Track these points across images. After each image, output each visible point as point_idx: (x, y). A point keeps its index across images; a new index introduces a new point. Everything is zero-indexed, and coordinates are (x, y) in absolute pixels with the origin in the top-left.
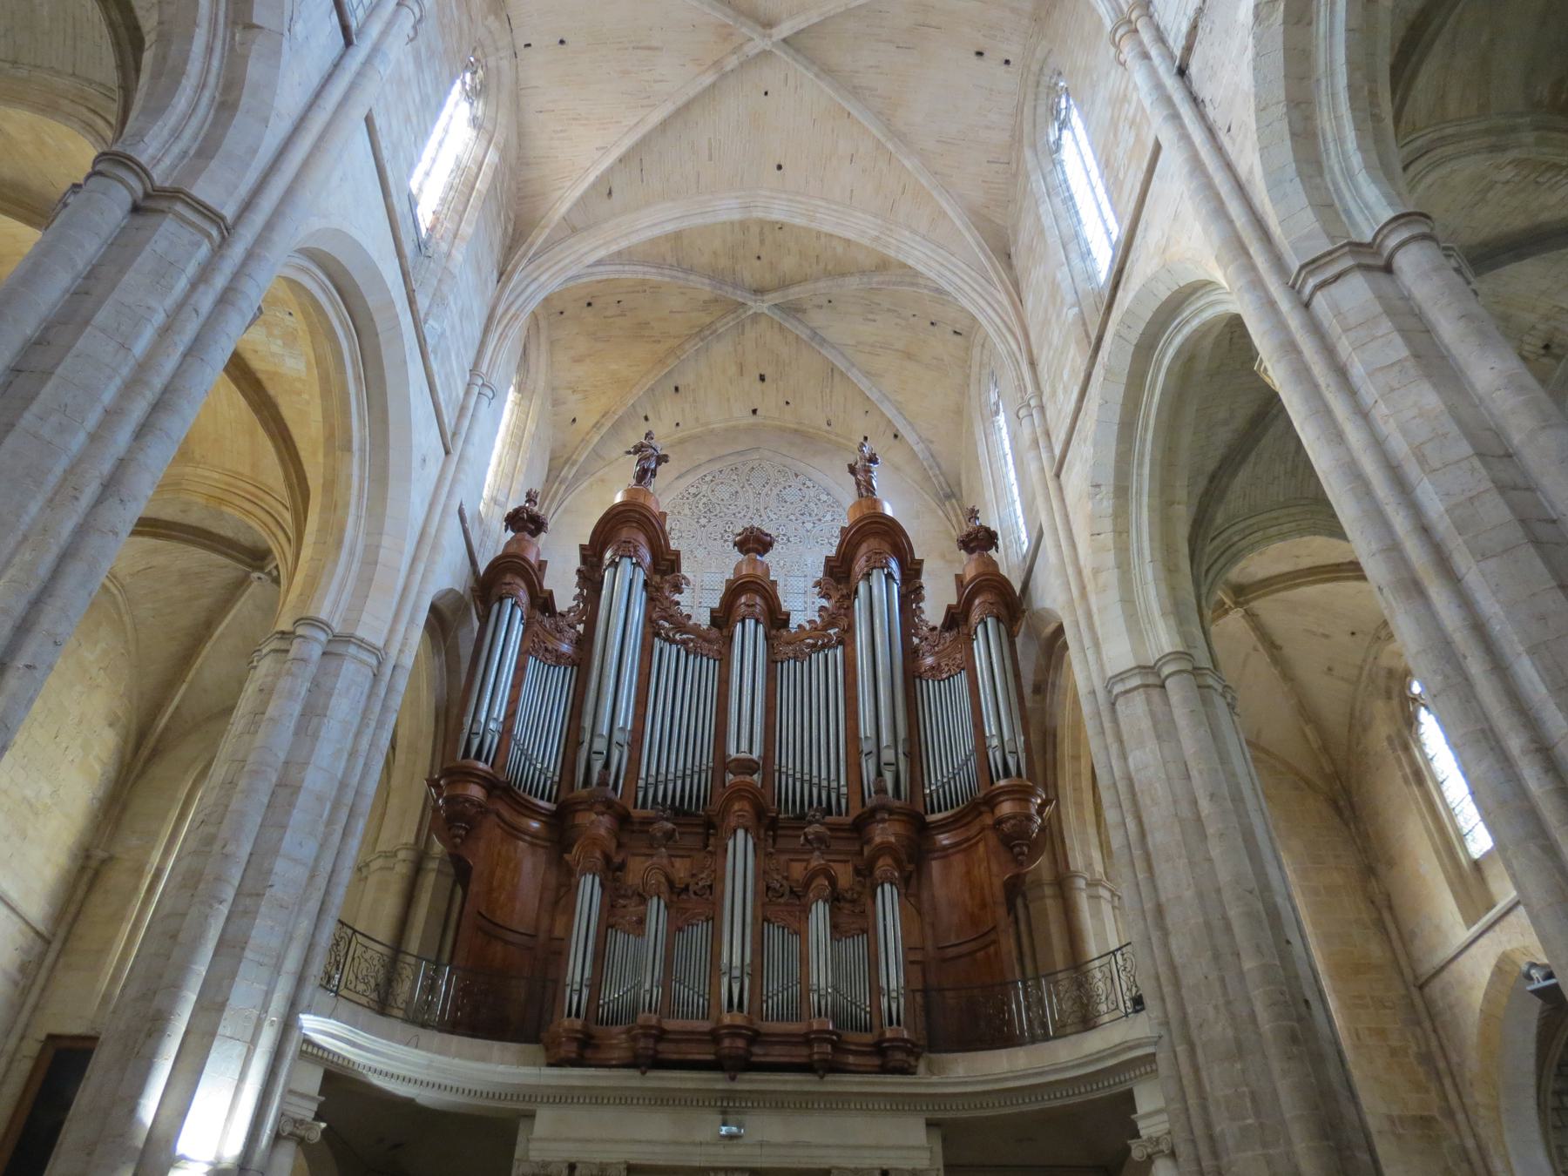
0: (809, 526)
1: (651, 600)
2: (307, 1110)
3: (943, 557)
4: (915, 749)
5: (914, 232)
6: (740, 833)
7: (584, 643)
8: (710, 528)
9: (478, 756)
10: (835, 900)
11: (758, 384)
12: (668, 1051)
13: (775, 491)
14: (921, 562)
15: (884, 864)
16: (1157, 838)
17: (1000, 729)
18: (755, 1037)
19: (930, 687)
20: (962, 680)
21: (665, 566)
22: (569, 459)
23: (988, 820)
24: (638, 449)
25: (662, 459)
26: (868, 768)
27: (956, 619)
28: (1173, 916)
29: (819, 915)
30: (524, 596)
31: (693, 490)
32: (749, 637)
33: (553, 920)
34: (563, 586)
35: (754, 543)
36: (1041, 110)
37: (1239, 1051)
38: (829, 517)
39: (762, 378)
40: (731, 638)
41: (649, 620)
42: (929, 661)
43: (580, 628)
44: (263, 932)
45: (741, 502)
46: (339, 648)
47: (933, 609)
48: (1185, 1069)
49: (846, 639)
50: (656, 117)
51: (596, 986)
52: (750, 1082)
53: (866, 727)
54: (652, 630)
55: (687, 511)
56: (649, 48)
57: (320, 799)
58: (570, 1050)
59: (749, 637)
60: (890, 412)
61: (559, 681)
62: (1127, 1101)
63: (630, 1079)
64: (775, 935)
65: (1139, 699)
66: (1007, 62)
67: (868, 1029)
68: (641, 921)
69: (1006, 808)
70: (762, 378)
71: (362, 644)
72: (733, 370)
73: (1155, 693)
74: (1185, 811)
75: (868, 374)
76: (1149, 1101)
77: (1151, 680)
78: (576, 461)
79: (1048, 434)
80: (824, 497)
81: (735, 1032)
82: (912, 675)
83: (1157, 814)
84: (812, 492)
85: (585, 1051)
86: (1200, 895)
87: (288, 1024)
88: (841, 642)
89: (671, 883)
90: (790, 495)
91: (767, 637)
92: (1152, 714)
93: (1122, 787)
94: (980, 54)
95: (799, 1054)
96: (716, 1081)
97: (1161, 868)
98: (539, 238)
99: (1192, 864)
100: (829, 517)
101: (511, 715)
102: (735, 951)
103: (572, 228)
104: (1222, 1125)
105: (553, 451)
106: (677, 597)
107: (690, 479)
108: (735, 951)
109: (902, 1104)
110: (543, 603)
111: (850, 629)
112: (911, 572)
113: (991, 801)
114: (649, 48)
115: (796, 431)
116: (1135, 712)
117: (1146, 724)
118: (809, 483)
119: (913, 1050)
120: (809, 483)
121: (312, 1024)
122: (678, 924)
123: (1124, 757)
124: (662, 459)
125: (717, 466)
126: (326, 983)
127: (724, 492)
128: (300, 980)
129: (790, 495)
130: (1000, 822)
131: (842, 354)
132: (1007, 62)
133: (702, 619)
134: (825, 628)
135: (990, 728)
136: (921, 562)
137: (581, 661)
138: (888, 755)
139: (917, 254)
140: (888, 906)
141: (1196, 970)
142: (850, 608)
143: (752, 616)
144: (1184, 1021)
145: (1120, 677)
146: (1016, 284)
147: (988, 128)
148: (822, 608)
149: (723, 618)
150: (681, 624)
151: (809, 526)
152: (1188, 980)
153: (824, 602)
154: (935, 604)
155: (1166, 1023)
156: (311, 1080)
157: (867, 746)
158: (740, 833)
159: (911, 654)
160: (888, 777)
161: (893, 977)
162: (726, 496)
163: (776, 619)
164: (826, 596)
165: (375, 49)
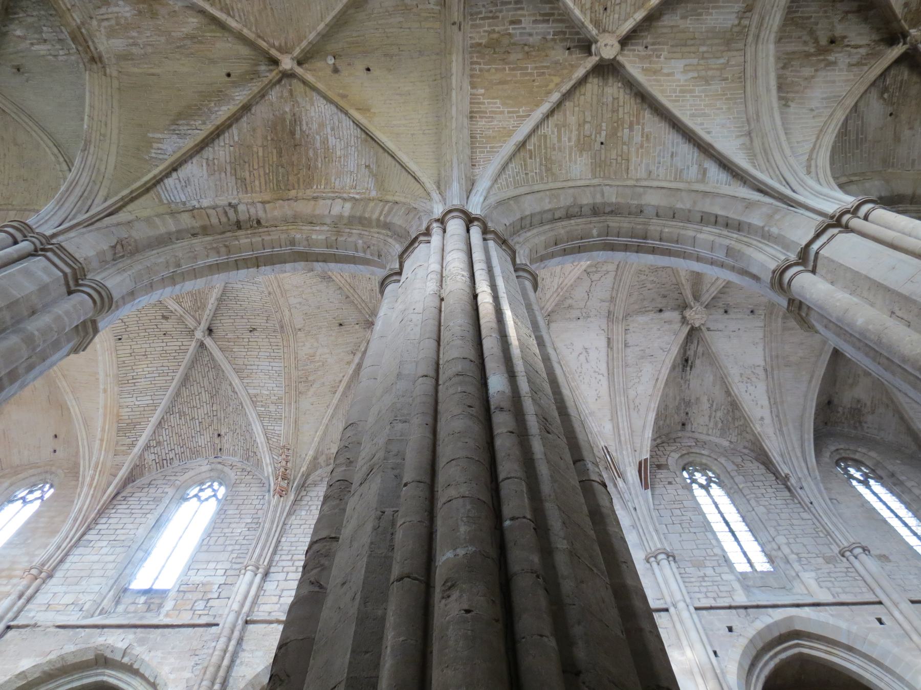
36: (33, 479)
66: (55, 451)
94: (56, 436)
132: (55, 451)
147: (19, 452)
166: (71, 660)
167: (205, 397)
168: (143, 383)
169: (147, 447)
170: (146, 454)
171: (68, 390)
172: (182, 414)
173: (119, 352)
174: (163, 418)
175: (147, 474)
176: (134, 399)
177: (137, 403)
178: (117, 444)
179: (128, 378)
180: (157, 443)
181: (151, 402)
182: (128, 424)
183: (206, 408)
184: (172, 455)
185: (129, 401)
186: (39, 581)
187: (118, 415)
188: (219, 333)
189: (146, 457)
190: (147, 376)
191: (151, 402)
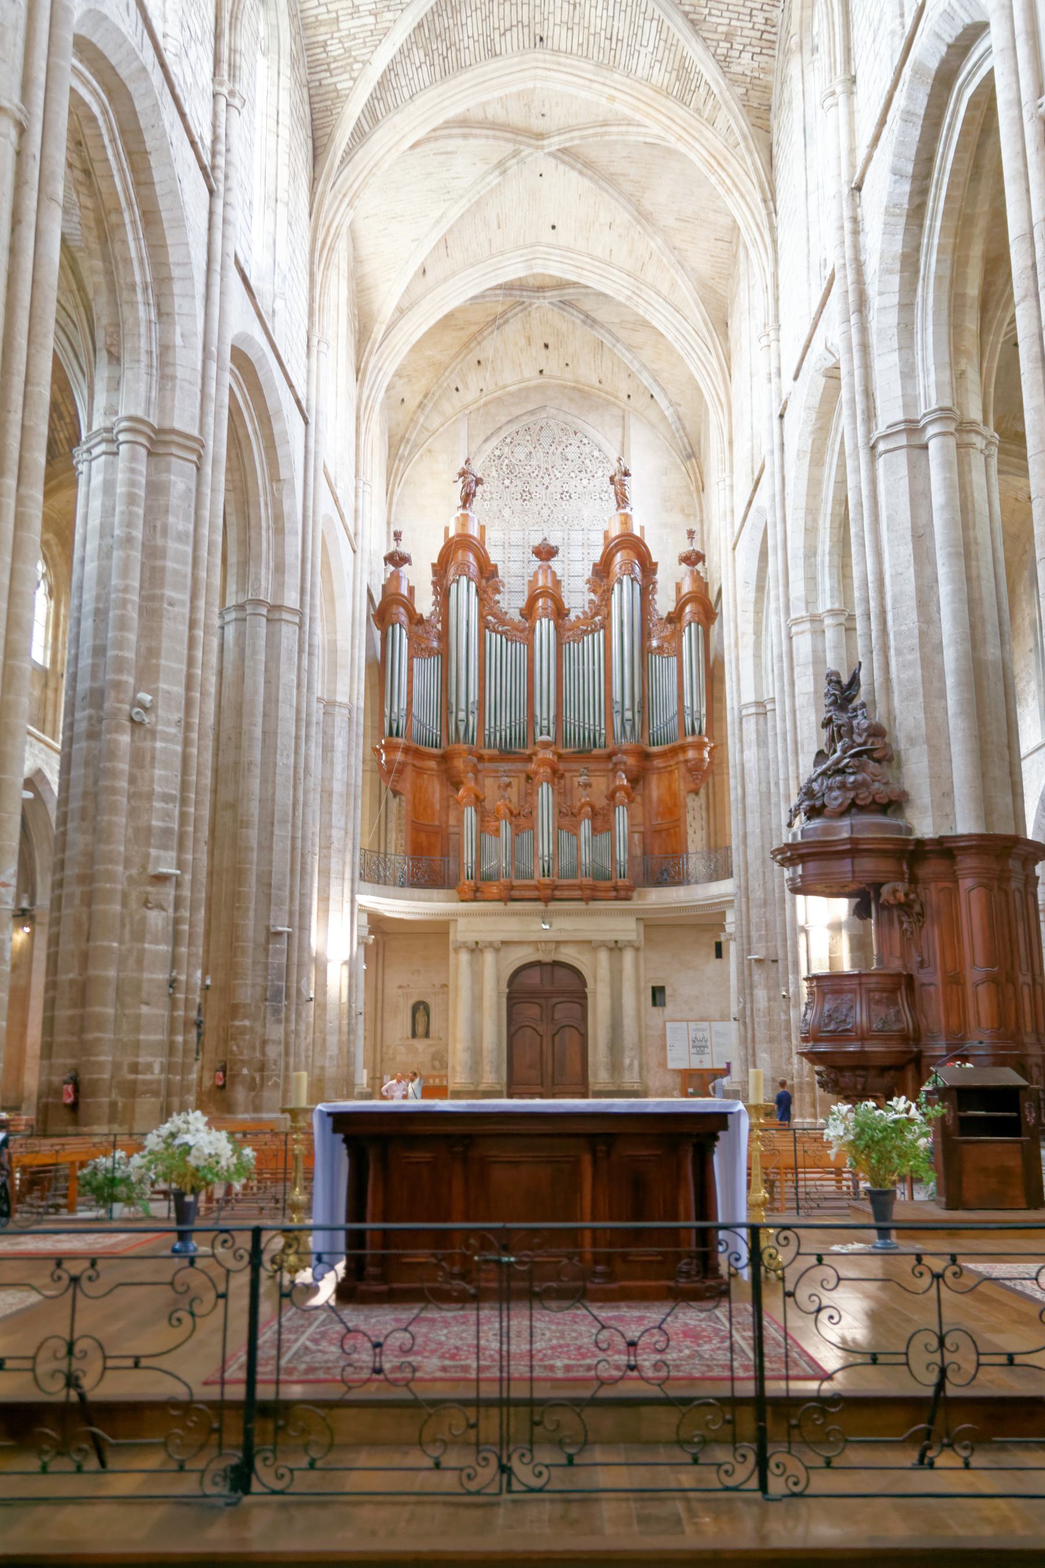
0: (585, 482)
1: (481, 600)
2: (365, 932)
3: (682, 510)
4: (645, 705)
5: (658, 293)
6: (545, 785)
7: (444, 636)
8: (512, 489)
9: (397, 734)
10: (594, 814)
11: (543, 350)
12: (515, 893)
13: (560, 450)
14: (656, 564)
15: (620, 795)
16: (749, 800)
17: (695, 702)
18: (556, 888)
19: (657, 661)
20: (674, 661)
22: (403, 437)
23: (681, 758)
24: (463, 474)
25: (479, 482)
27: (675, 618)
28: (750, 840)
29: (585, 827)
30: (404, 619)
31: (497, 453)
32: (544, 628)
33: (448, 815)
34: (425, 605)
35: (546, 553)
37: (765, 903)
38: (600, 474)
39: (546, 346)
40: (534, 630)
41: (481, 617)
42: (655, 643)
43: (439, 626)
44: (335, 865)
45: (534, 463)
46: (276, 616)
47: (664, 603)
48: (744, 909)
49: (606, 625)
50: (455, 213)
51: (478, 863)
52: (553, 906)
53: (617, 696)
54: (484, 625)
55: (494, 474)
56: (447, 153)
57: (341, 796)
58: (470, 895)
59: (544, 628)
60: (646, 380)
61: (432, 664)
62: (723, 914)
63: (498, 906)
64: (564, 834)
65: (753, 720)
67: (610, 879)
68: (497, 830)
69: (691, 754)
70: (546, 346)
71: (341, 705)
72: (523, 342)
73: (761, 718)
74: (764, 789)
75: (629, 348)
76: (730, 917)
77: (761, 710)
78: (408, 440)
79: (732, 511)
80: (596, 453)
81: (546, 886)
82: (645, 651)
83: (752, 787)
84: (587, 449)
85: (476, 895)
86: (762, 832)
87: (353, 901)
88: (603, 627)
89: (511, 813)
90: (572, 452)
91: (556, 627)
92: (758, 731)
93: (738, 768)
95: (577, 893)
96: (539, 906)
97: (749, 815)
98: (378, 331)
99: (761, 816)
100: (600, 474)
101: (410, 703)
102: (545, 847)
103: (401, 312)
104: (754, 934)
105: (390, 430)
106: (497, 597)
107: (495, 442)
108: (545, 847)
109: (624, 913)
110: (416, 620)
111: (608, 617)
112: (649, 568)
113: (683, 748)
114: (447, 153)
115: (574, 388)
116: (750, 727)
117: (754, 737)
118: (585, 441)
119: (630, 889)
120: (585, 441)
121: (362, 899)
122: (517, 831)
123: (742, 751)
124: (479, 482)
125: (514, 427)
126: (362, 878)
127: (520, 453)
128: (353, 880)
129: (572, 452)
130: (686, 761)
131: (610, 332)
133: (515, 615)
134: (593, 617)
135: (687, 703)
136: (656, 564)
137: (444, 655)
138: (628, 715)
139: (660, 318)
140: (621, 818)
141: (755, 866)
142: (609, 599)
143: (546, 616)
144: (747, 888)
145: (746, 706)
146: (728, 359)
147: (715, 211)
148: (591, 602)
149: (529, 612)
151: (585, 482)
152: (751, 871)
153: (592, 596)
154: (664, 603)
155: (739, 887)
156: (364, 919)
157: (617, 707)
158: (545, 785)
159: (646, 635)
160: (628, 728)
161: (621, 855)
162: (523, 458)
163: (560, 613)
164: (594, 591)
165: (317, 411)
166: (815, 401)
168: (621, 27)
169: (724, 63)
170: (735, 68)
171: (624, 129)
173: (563, 48)
174: (686, 14)
175: (770, 78)
176: (643, 51)
177: (650, 48)
178: (698, 111)
179: (607, 48)
180: (726, 40)
181: (655, 23)
182: (678, 79)
185: (644, 61)
186: (773, 344)
187: (658, 90)
189: (739, 69)
190: (611, 13)
191: (655, 23)
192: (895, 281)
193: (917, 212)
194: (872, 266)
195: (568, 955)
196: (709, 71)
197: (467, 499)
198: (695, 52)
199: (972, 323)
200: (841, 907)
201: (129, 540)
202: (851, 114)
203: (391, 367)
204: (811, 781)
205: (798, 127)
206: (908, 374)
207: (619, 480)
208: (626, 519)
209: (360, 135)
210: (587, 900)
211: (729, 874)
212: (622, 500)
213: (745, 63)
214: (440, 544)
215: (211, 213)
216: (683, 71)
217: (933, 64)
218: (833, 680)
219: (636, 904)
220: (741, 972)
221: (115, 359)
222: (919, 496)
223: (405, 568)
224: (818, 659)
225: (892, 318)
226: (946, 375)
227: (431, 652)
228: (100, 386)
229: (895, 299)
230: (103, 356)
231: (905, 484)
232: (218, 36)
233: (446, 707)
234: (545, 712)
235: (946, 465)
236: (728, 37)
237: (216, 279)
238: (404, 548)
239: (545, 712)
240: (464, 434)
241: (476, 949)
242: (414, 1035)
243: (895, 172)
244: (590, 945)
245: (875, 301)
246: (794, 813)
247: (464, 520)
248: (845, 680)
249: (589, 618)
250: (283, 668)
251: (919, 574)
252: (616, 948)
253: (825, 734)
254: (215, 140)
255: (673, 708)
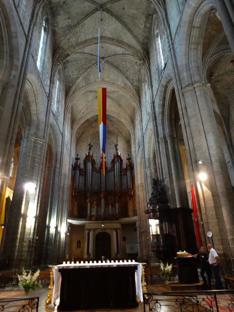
4: (121, 184)
7: (85, 172)
21: (93, 162)
24: (89, 145)
25: (92, 146)
26: (116, 187)
27: (126, 169)
34: (82, 167)
47: (124, 166)
49: (114, 170)
62: (136, 223)
76: (137, 223)
82: (121, 175)
109: (118, 223)
110: (80, 170)
112: (121, 161)
124: (92, 146)
137: (85, 176)
139: (123, 120)
150: (96, 169)
154: (124, 166)
159: (121, 172)
161: (117, 211)
167: (124, 63)
169: (132, 84)
170: (134, 84)
172: (127, 71)
183: (127, 64)
184: (137, 77)
188: (104, 56)
192: (161, 116)
193: (163, 105)
194: (157, 113)
195: (107, 231)
196: (129, 84)
197: (90, 149)
198: (127, 82)
199: (173, 122)
200: (157, 221)
201: (30, 155)
202: (152, 91)
203: (77, 127)
204: (151, 198)
205: (144, 92)
206: (164, 130)
207: (116, 146)
208: (117, 153)
209: (74, 93)
210: (110, 220)
211: (137, 215)
212: (117, 149)
213: (135, 83)
214: (85, 156)
215: (48, 103)
216: (125, 84)
217: (164, 84)
218: (154, 180)
219: (120, 221)
220: (139, 234)
221: (30, 126)
222: (167, 149)
223: (79, 161)
224: (151, 176)
225: (161, 121)
226: (170, 130)
227: (83, 175)
228: (26, 130)
229: (161, 118)
230: (28, 125)
231: (164, 147)
232: (51, 78)
233: (85, 184)
234: (103, 185)
235: (171, 144)
236: (133, 80)
237: (48, 114)
238: (79, 157)
239: (103, 185)
240: (90, 139)
241: (90, 230)
242: (77, 247)
243: (160, 100)
244: (111, 229)
245: (158, 118)
246: (148, 204)
247: (89, 153)
248: (156, 180)
249: (111, 169)
250: (56, 178)
251: (168, 162)
252: (116, 230)
253: (153, 190)
254: (49, 92)
255: (126, 185)
